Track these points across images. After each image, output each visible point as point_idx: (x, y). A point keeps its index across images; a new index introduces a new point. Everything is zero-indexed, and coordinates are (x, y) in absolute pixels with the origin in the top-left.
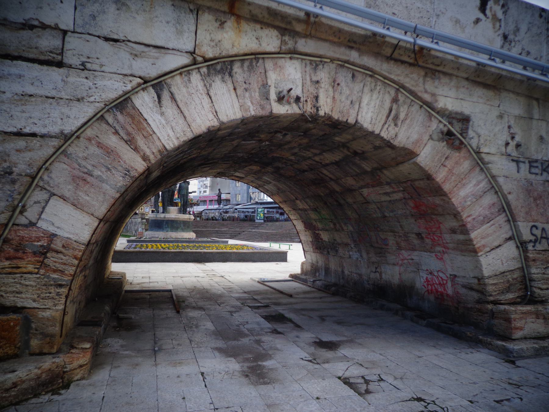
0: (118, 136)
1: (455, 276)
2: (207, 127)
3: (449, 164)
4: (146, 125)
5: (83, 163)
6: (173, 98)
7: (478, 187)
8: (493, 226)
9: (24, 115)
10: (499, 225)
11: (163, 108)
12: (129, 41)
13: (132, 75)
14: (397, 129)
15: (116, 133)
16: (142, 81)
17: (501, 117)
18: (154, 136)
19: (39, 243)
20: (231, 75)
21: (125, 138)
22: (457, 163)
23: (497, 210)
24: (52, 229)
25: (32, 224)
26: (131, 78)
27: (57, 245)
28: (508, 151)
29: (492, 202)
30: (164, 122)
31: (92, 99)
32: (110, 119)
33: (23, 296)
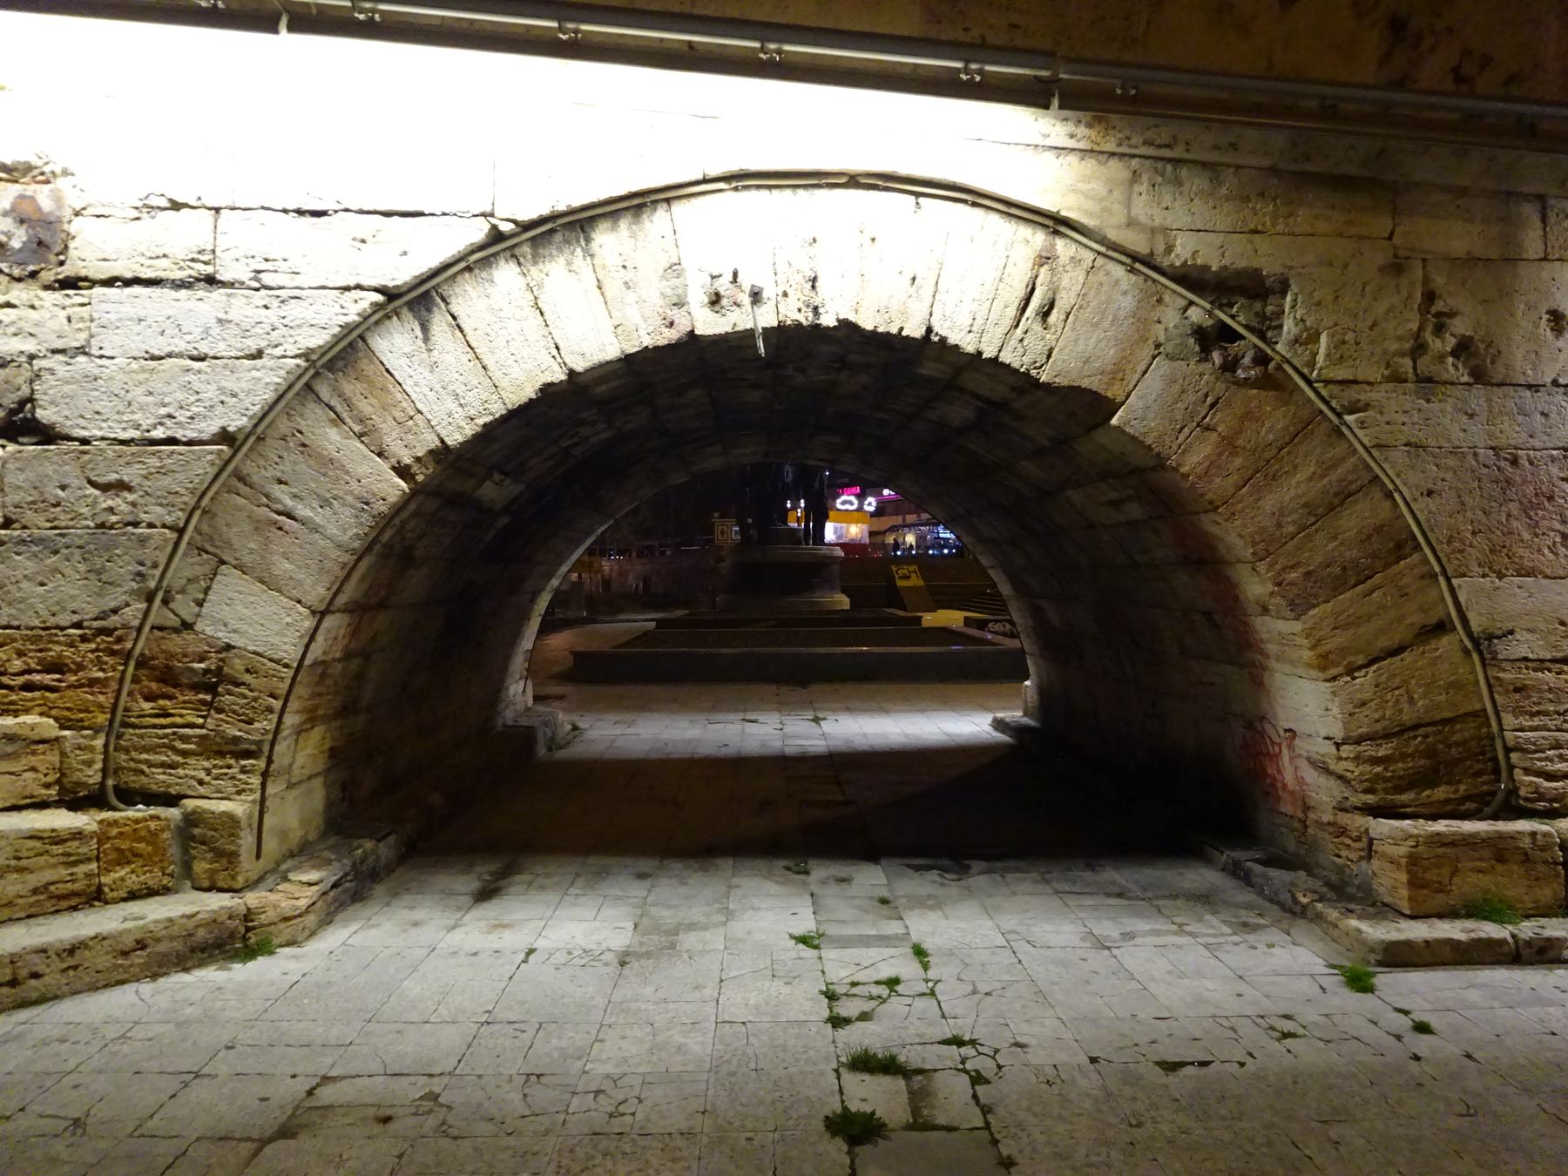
2: (538, 385)
4: (399, 396)
7: (1325, 481)
9: (150, 399)
11: (435, 353)
12: (347, 210)
13: (359, 287)
16: (379, 298)
17: (1396, 267)
19: (202, 666)
24: (224, 636)
25: (187, 626)
27: (237, 666)
31: (278, 352)
32: (324, 391)
33: (181, 772)
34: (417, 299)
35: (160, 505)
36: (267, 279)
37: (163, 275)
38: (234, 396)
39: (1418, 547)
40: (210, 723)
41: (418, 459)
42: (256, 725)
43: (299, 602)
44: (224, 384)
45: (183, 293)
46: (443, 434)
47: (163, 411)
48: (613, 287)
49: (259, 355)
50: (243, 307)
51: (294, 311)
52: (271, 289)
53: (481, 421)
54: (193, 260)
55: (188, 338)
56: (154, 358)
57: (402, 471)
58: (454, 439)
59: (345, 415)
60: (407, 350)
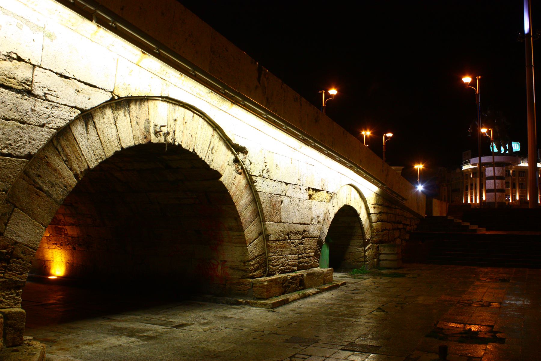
1: (225, 261)
2: (114, 151)
4: (78, 148)
9: (4, 136)
11: (89, 135)
12: (75, 79)
21: (64, 158)
26: (74, 110)
31: (50, 126)
32: (55, 143)
34: (87, 116)
35: (3, 182)
36: (49, 97)
37: (14, 86)
38: (34, 140)
40: (7, 276)
41: (81, 172)
42: (24, 275)
43: (42, 224)
44: (31, 135)
45: (19, 95)
46: (89, 164)
47: (8, 142)
48: (134, 123)
49: (43, 126)
50: (40, 106)
51: (57, 112)
52: (49, 101)
53: (99, 161)
54: (24, 83)
55: (20, 114)
56: (6, 119)
57: (76, 176)
58: (92, 166)
60: (81, 132)
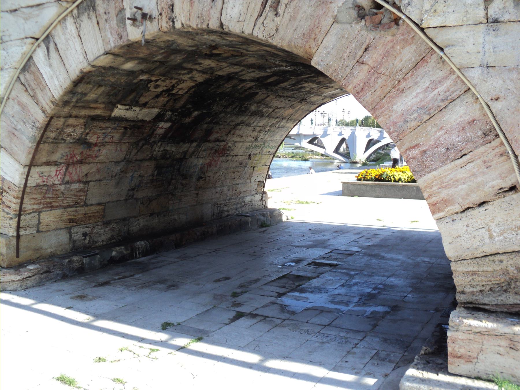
0: (27, 93)
2: (79, 70)
3: (371, 58)
5: (12, 119)
6: (57, 49)
7: (436, 92)
8: (471, 165)
10: (485, 162)
11: (51, 60)
14: (277, 19)
15: (27, 90)
18: (47, 88)
20: (94, 9)
22: (387, 55)
23: (480, 133)
28: (491, 12)
29: (467, 118)
30: (52, 73)
39: (497, 136)
59: (28, 89)
